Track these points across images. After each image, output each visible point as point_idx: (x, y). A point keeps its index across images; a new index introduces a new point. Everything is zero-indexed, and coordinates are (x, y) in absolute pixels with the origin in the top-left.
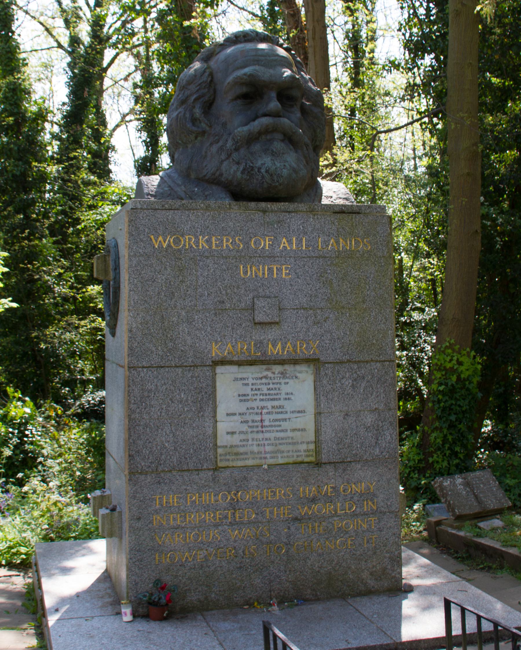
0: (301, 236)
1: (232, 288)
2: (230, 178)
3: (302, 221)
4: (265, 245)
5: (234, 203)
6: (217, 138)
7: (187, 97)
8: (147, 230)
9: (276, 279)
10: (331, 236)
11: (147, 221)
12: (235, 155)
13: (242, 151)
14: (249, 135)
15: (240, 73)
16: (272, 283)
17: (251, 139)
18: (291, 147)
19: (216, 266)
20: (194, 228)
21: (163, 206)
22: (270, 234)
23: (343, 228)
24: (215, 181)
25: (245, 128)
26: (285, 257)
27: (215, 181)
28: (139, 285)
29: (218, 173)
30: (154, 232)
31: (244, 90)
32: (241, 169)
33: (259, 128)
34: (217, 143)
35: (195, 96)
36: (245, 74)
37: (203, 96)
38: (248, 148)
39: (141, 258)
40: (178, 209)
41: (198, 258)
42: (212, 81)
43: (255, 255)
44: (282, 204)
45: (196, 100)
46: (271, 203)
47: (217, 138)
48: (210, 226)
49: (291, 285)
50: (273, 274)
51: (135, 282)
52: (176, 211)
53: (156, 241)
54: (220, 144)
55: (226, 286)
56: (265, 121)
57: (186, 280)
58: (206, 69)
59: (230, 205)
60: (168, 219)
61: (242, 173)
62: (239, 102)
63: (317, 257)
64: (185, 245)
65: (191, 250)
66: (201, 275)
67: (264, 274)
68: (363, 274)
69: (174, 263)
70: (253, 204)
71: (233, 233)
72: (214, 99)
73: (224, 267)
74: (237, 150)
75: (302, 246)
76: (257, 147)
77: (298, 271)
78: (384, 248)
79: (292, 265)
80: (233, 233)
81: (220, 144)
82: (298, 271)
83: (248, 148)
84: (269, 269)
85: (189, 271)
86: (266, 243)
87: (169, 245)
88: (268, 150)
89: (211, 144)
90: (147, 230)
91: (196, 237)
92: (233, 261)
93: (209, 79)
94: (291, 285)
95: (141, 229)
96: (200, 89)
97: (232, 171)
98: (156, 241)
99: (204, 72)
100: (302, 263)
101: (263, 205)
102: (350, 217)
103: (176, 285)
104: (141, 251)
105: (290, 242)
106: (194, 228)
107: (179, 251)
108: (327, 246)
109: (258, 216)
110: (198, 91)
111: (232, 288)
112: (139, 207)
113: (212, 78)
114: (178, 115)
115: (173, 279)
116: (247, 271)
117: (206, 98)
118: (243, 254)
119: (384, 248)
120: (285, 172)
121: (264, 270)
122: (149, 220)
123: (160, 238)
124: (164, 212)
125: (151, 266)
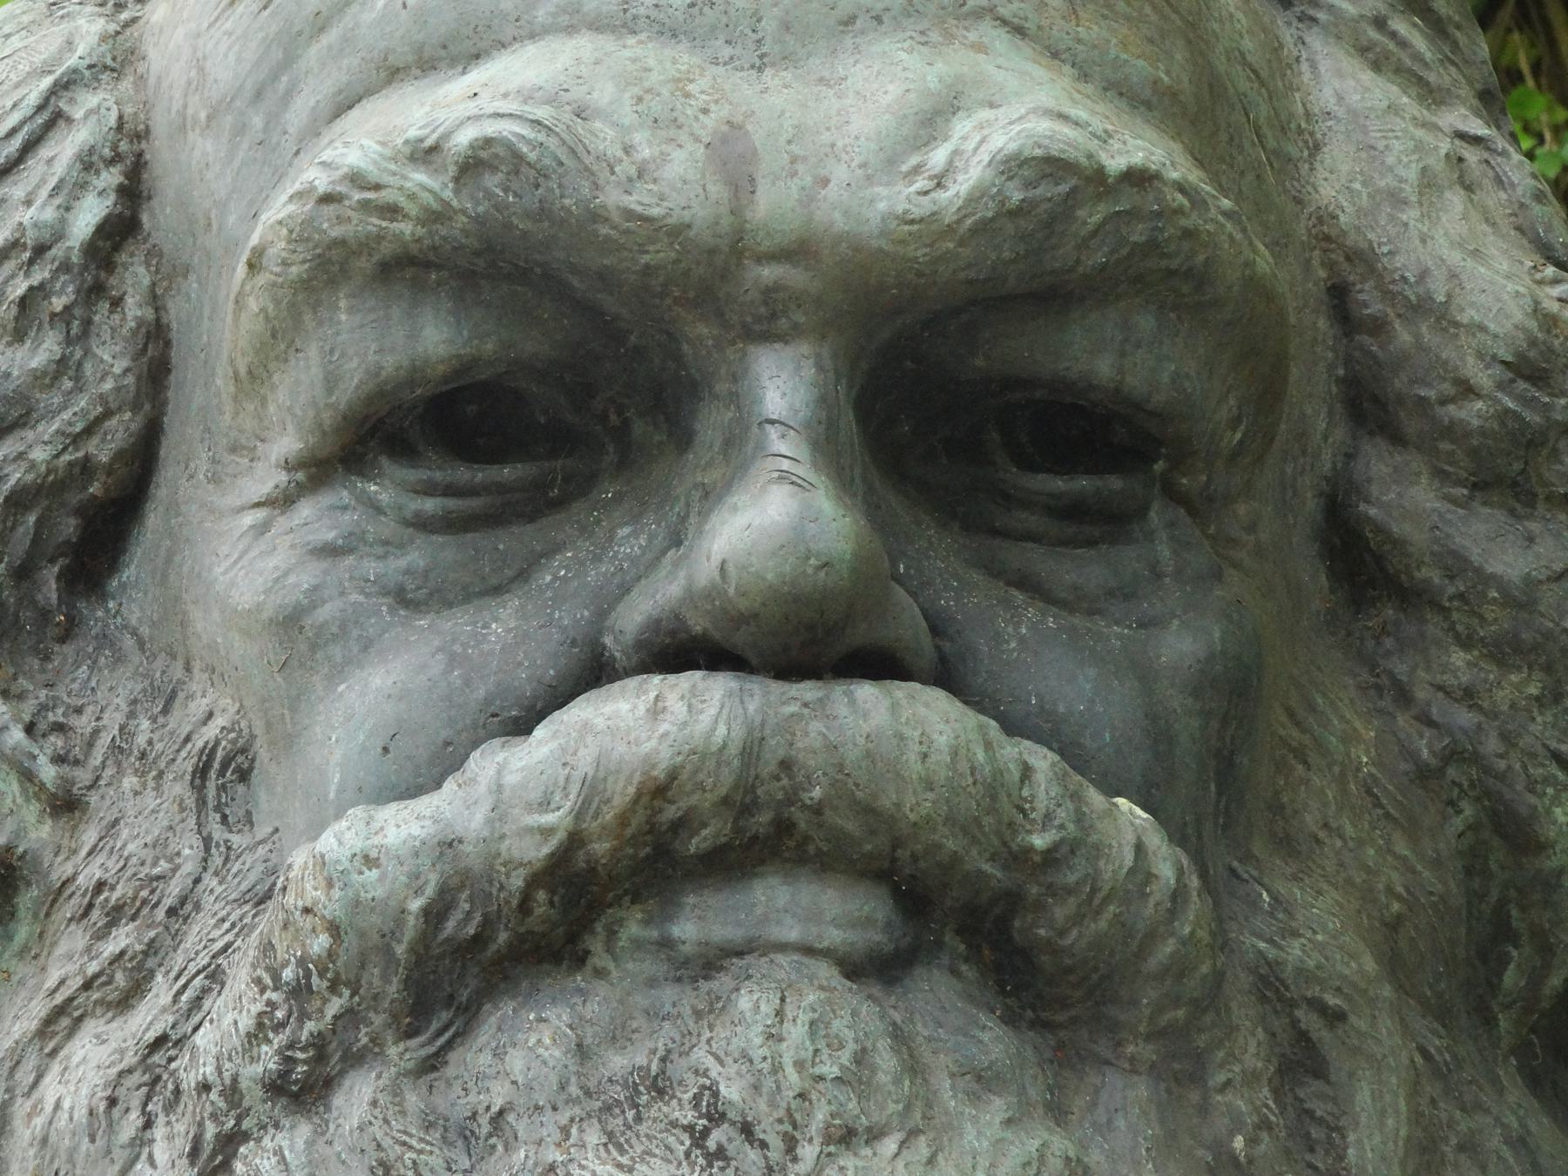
6: (123, 938)
14: (435, 914)
18: (994, 1042)
25: (403, 825)
31: (432, 338)
34: (123, 1004)
36: (425, 154)
42: (120, 231)
47: (123, 938)
54: (149, 1017)
56: (645, 725)
58: (66, 85)
62: (388, 489)
72: (144, 457)
74: (303, 1089)
81: (149, 1017)
83: (431, 1065)
88: (660, 1088)
89: (62, 1021)
93: (88, 215)
99: (50, 118)
113: (133, 193)
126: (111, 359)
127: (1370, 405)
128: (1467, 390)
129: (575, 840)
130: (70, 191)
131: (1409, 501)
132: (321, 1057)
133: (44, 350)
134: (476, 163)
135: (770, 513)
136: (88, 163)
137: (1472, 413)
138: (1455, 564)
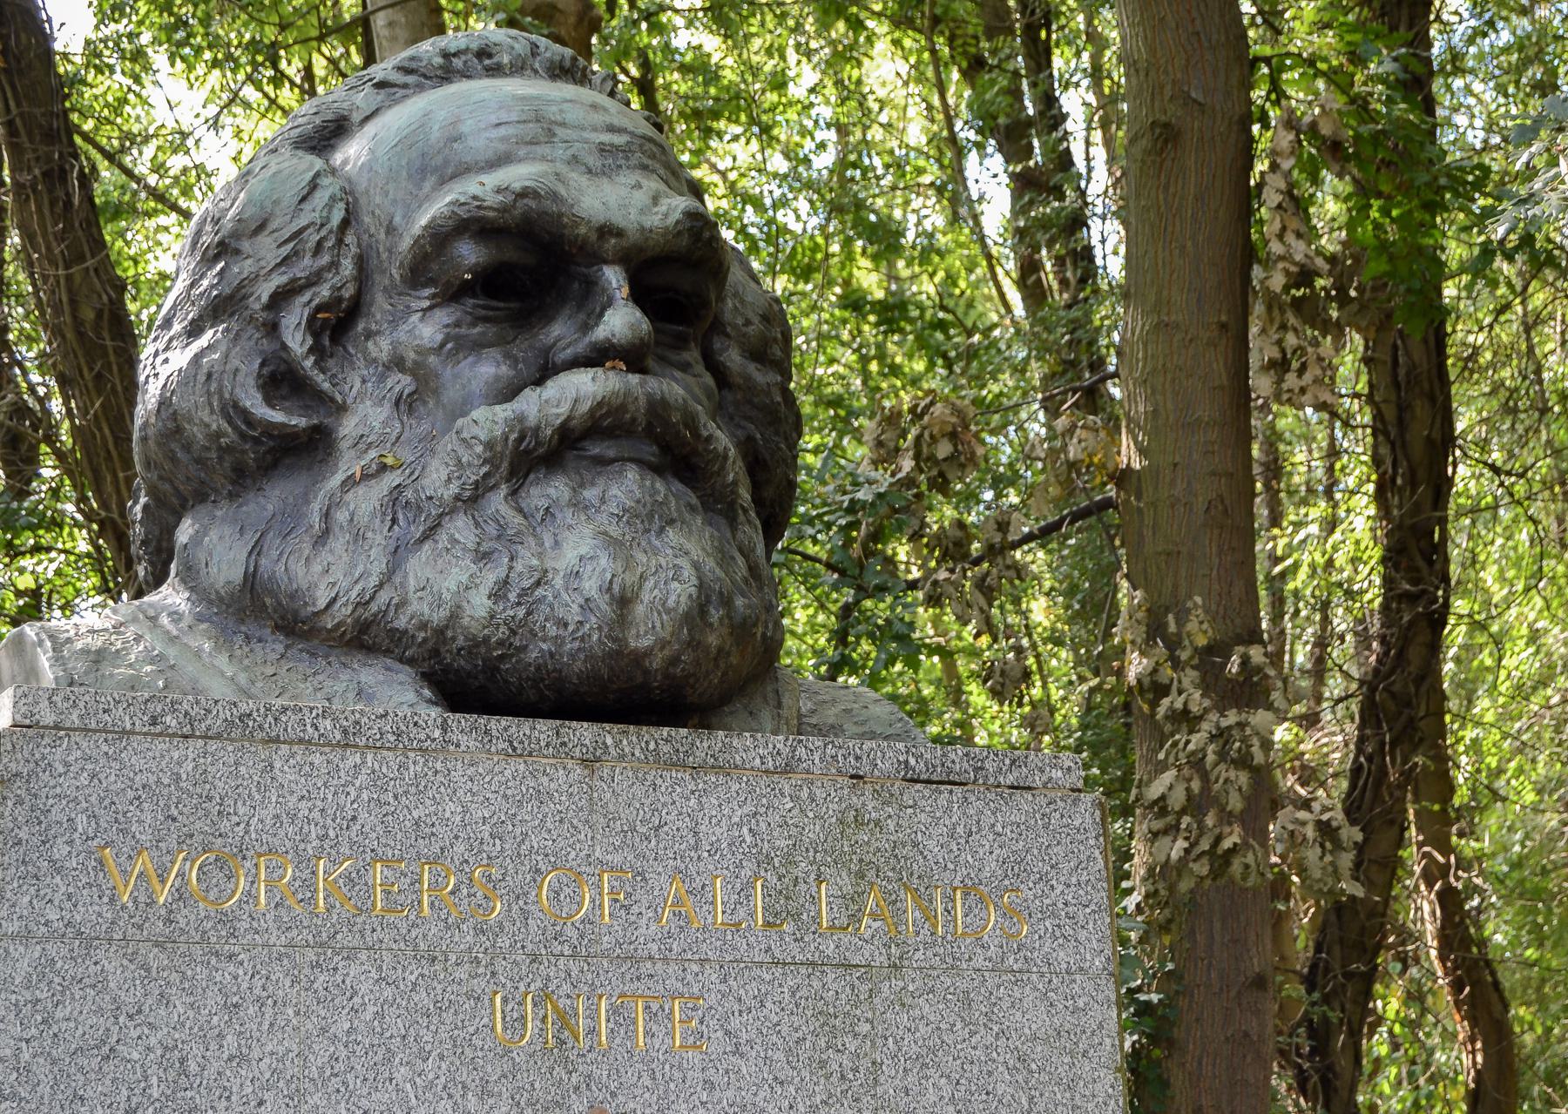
0: (746, 872)
1: (457, 1093)
2: (438, 617)
3: (749, 809)
4: (597, 905)
5: (460, 721)
7: (240, 287)
8: (81, 821)
9: (647, 1060)
10: (871, 874)
11: (84, 779)
12: (461, 528)
13: (497, 501)
15: (484, 188)
16: (630, 1077)
17: (532, 457)
19: (388, 992)
20: (293, 818)
21: (154, 721)
22: (617, 859)
23: (915, 845)
24: (366, 637)
25: (503, 412)
26: (682, 961)
27: (366, 637)
28: (41, 1068)
29: (383, 597)
30: (113, 834)
32: (490, 577)
33: (564, 410)
35: (278, 280)
37: (314, 280)
38: (514, 493)
39: (52, 950)
40: (218, 736)
41: (311, 955)
42: (345, 223)
43: (557, 949)
44: (665, 731)
45: (281, 298)
46: (616, 728)
48: (363, 816)
49: (709, 1085)
50: (631, 1035)
51: (26, 1056)
52: (213, 746)
53: (125, 873)
55: (431, 1085)
57: (256, 1054)
59: (445, 728)
60: (178, 778)
61: (498, 594)
63: (813, 964)
64: (250, 896)
65: (277, 918)
66: (324, 1030)
67: (593, 1031)
68: (1002, 1042)
69: (201, 973)
70: (543, 729)
71: (460, 848)
73: (421, 997)
75: (752, 914)
76: (552, 490)
77: (735, 1022)
78: (1083, 935)
79: (713, 999)
80: (460, 848)
82: (735, 1022)
84: (614, 1011)
85: (269, 1011)
86: (595, 901)
87: (180, 895)
90: (81, 821)
91: (301, 861)
92: (461, 973)
93: (337, 216)
94: (709, 1085)
95: (55, 815)
96: (295, 253)
97: (451, 584)
98: (125, 873)
99: (313, 186)
100: (753, 988)
101: (584, 733)
102: (943, 800)
103: (210, 1073)
104: (53, 915)
105: (700, 893)
106: (293, 818)
107: (225, 919)
108: (855, 918)
109: (564, 778)
110: (285, 261)
111: (457, 1093)
112: (49, 718)
114: (197, 358)
115: (197, 1050)
116: (523, 1018)
117: (324, 292)
118: (504, 942)
119: (1083, 935)
120: (681, 593)
121: (593, 1015)
122: (93, 776)
123: (142, 863)
124: (160, 746)
125: (100, 984)
126: (348, 267)
127: (718, 326)
128: (748, 323)
129: (569, 419)
130: (329, 206)
131: (733, 358)
132: (476, 488)
133: (325, 259)
134: (524, 194)
135: (621, 320)
136: (333, 198)
137: (751, 330)
138: (748, 378)
